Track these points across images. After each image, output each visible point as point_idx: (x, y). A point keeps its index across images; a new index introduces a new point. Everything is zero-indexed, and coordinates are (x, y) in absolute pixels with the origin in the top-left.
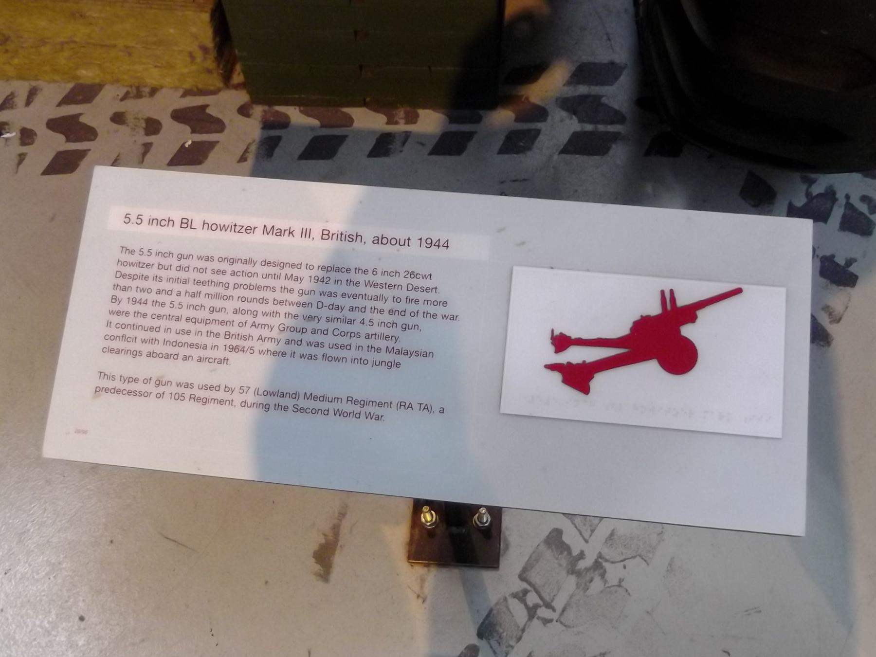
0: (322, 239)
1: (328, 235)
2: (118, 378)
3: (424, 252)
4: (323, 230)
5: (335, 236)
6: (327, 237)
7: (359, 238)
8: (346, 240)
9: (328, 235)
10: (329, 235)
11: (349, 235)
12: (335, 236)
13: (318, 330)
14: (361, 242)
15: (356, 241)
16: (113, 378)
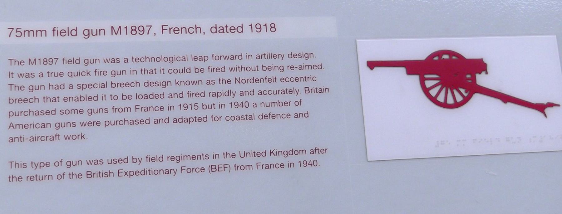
2: (29, 165)
3: (255, 36)
13: (160, 120)
14: (201, 33)
16: (24, 166)
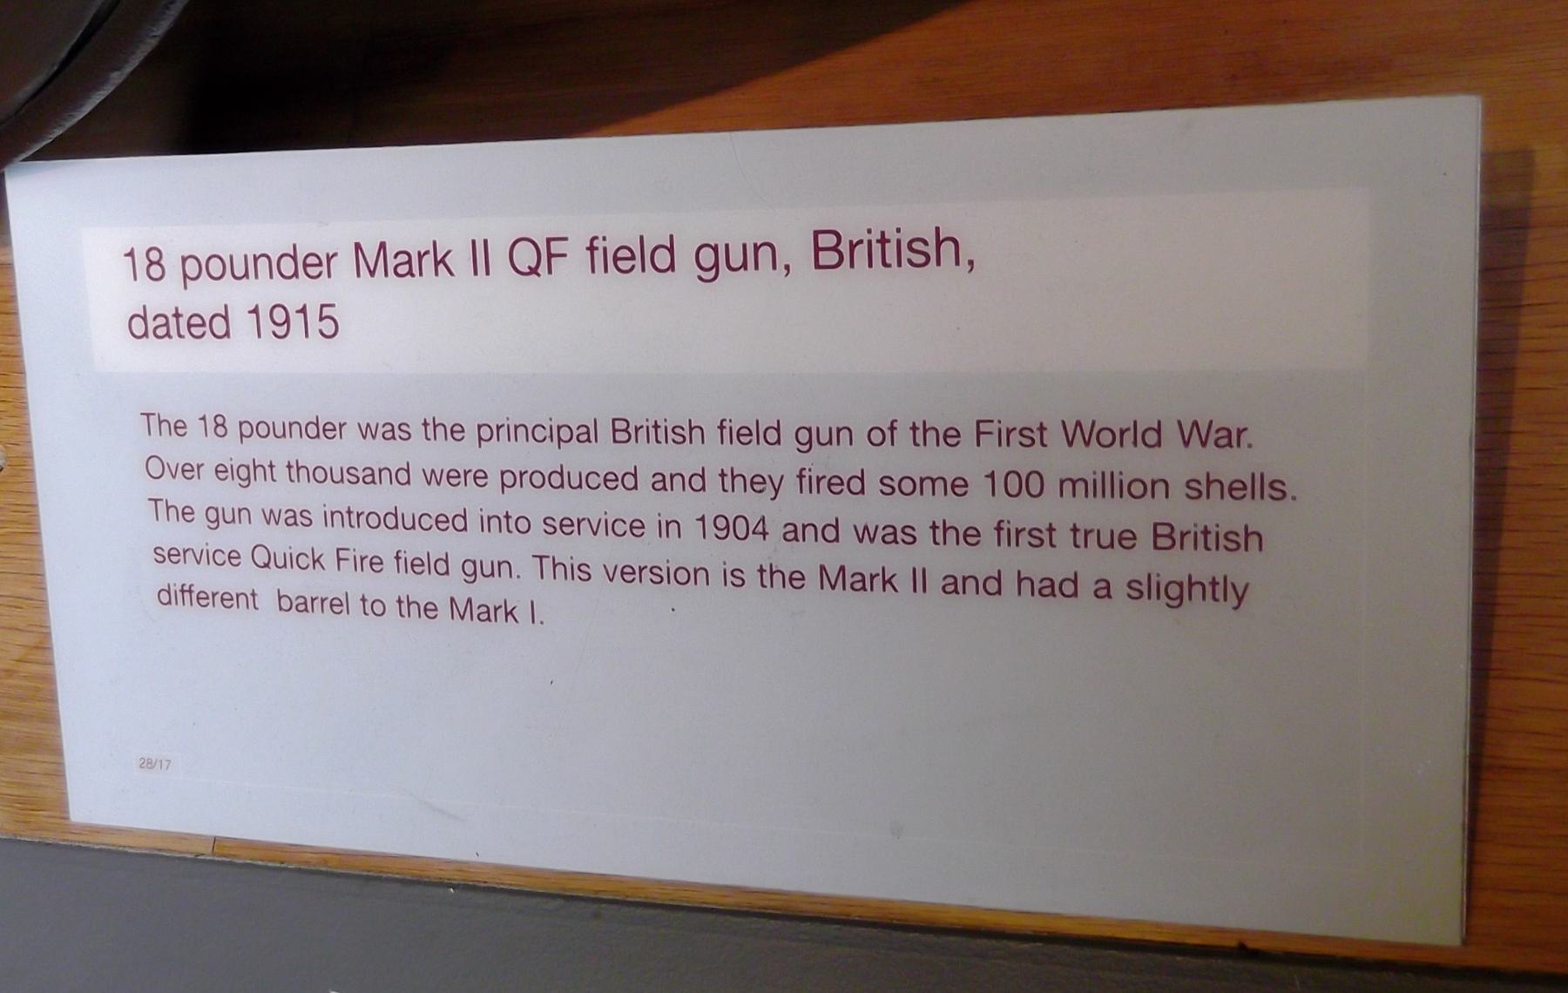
0: (818, 266)
1: (835, 249)
4: (816, 233)
5: (861, 251)
6: (832, 258)
7: (947, 248)
8: (904, 261)
9: (835, 249)
10: (840, 248)
11: (911, 242)
12: (861, 251)
15: (938, 263)
